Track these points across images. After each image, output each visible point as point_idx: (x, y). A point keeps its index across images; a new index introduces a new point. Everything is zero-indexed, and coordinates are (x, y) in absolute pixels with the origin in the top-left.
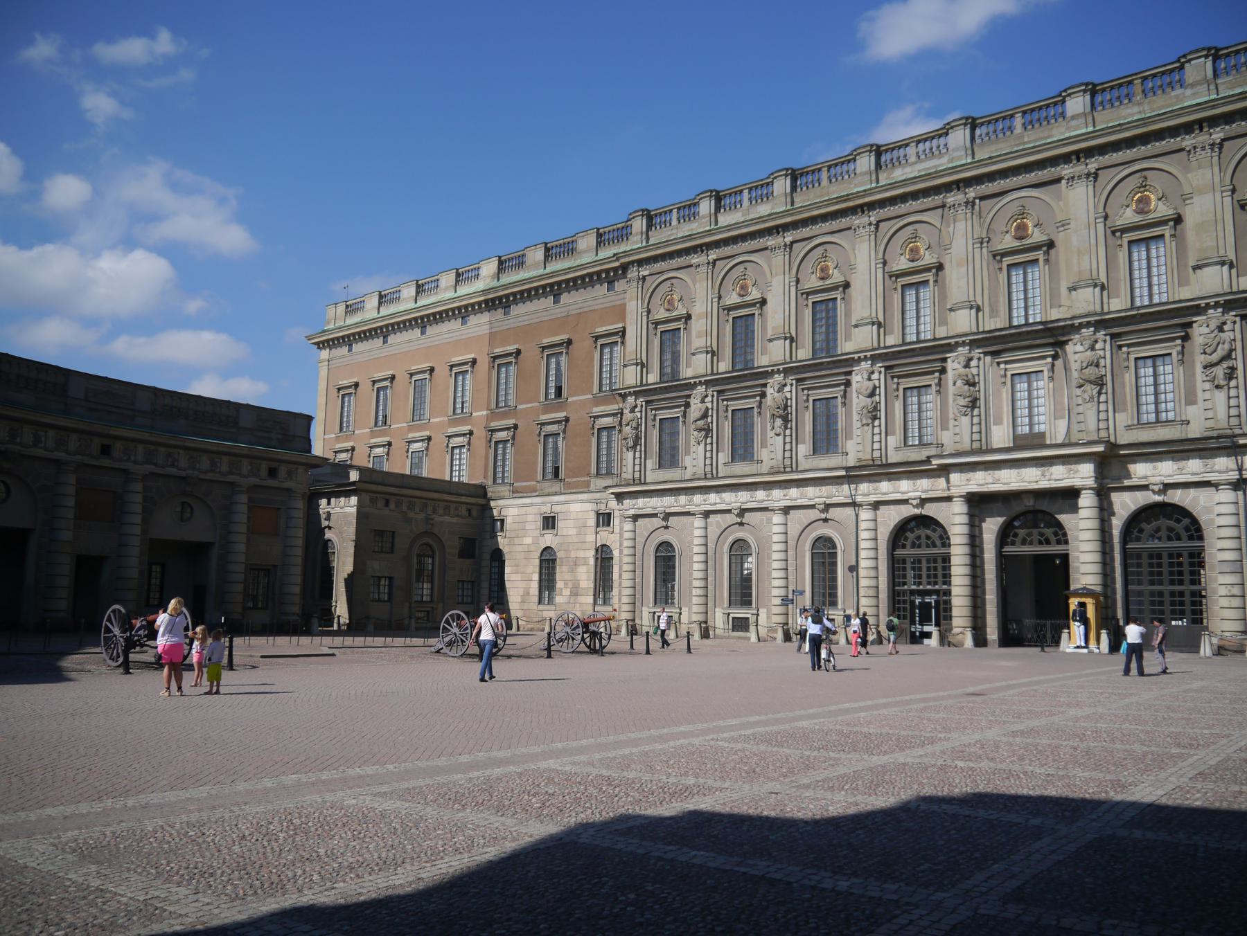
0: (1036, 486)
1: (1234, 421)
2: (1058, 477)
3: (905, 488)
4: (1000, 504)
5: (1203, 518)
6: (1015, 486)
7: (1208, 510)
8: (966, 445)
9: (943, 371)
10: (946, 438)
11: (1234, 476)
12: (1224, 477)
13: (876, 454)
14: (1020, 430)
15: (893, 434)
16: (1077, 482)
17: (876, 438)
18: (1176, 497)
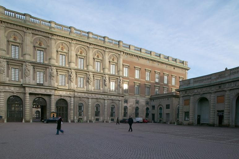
0: (43, 93)
1: (73, 88)
2: (48, 92)
3: (12, 89)
4: (34, 96)
5: (69, 102)
6: (40, 93)
7: (69, 101)
8: (27, 82)
9: (22, 66)
10: (21, 80)
11: (73, 96)
12: (72, 96)
13: (4, 81)
14: (37, 82)
15: (9, 77)
16: (51, 94)
17: (4, 77)
18: (65, 98)
